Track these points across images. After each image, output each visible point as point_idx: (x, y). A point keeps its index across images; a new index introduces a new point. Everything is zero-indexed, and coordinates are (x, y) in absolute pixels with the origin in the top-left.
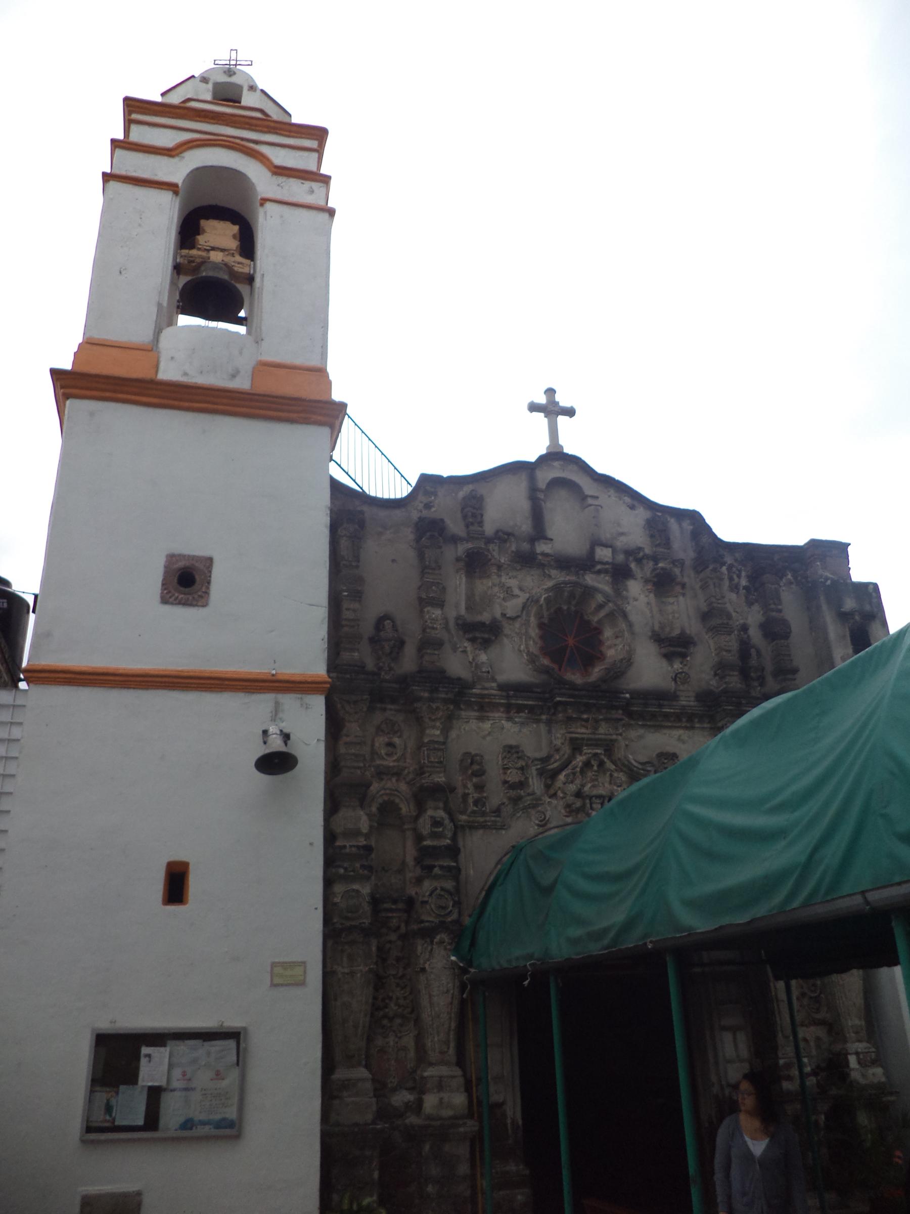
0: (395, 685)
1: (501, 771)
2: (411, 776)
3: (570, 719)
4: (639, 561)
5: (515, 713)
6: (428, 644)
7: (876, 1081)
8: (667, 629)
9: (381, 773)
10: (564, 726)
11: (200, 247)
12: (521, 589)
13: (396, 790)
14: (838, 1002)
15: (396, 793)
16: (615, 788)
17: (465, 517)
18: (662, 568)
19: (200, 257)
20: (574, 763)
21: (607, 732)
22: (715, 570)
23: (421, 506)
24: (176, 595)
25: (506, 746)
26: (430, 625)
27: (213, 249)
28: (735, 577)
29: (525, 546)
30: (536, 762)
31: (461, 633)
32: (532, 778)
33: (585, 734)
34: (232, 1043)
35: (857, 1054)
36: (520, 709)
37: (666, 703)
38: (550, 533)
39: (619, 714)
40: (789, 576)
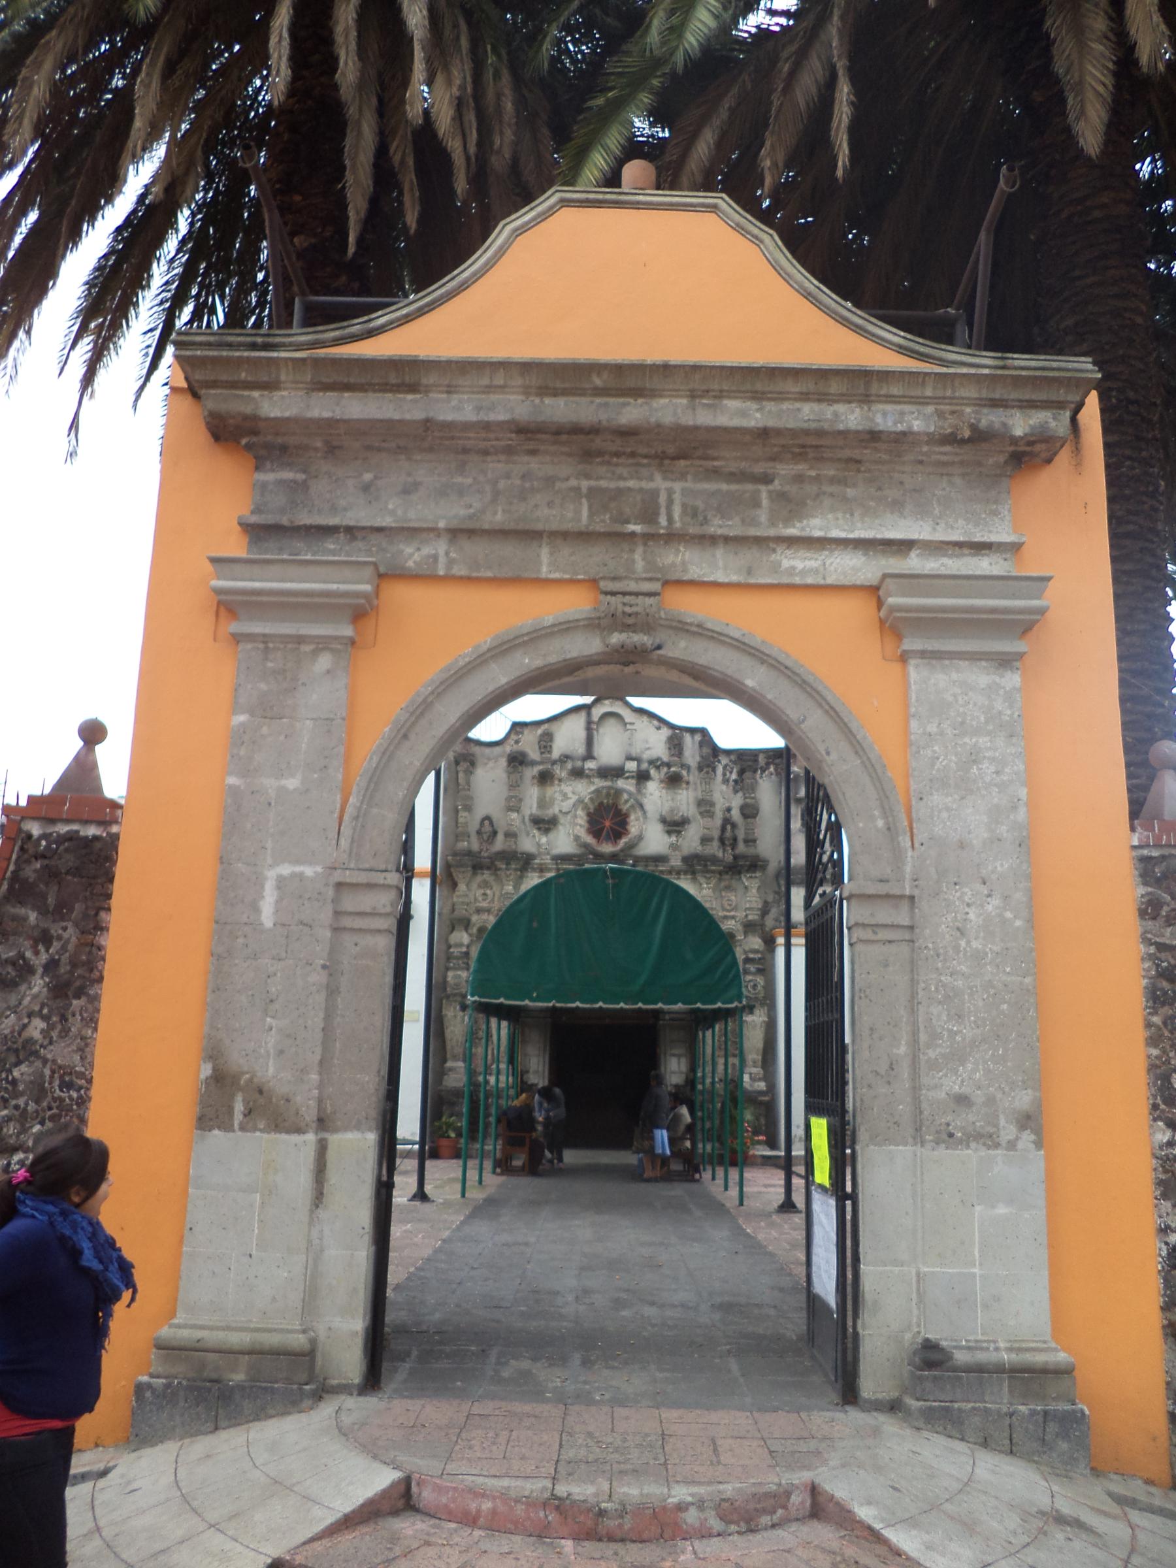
4: (658, 768)
9: (479, 911)
12: (574, 793)
29: (579, 764)
38: (595, 754)
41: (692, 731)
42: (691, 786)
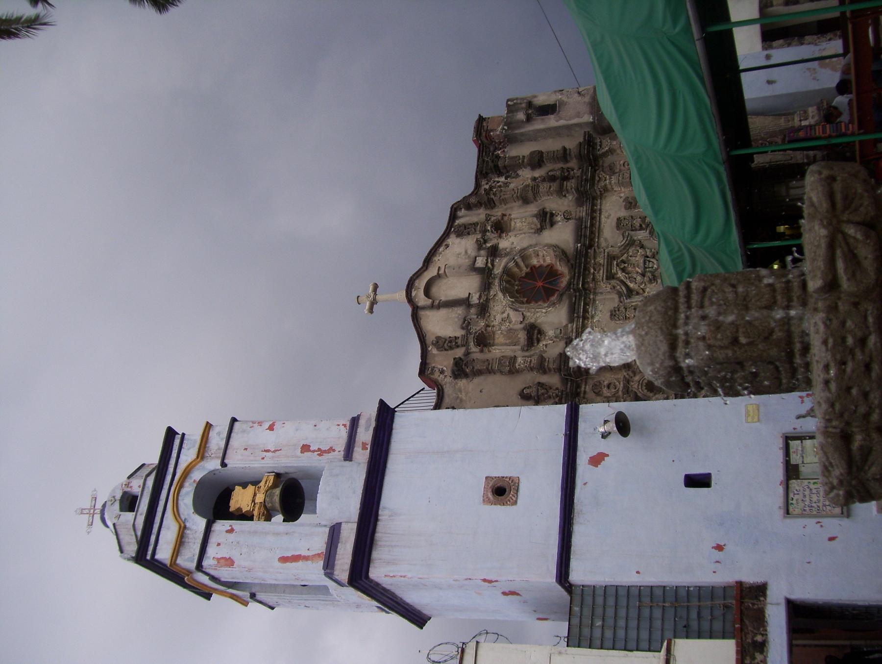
0: (569, 385)
1: (627, 321)
2: (630, 373)
3: (594, 279)
4: (485, 242)
5: (589, 314)
6: (542, 367)
7: (816, 112)
8: (533, 226)
10: (599, 283)
11: (251, 510)
12: (503, 313)
13: (639, 382)
14: (771, 130)
15: (641, 382)
16: (639, 254)
17: (451, 348)
18: (491, 227)
19: (259, 509)
20: (622, 278)
21: (603, 258)
22: (495, 194)
23: (441, 376)
24: (511, 496)
25: (611, 319)
26: (528, 364)
27: (253, 501)
28: (498, 184)
29: (473, 311)
30: (622, 299)
31: (533, 348)
32: (632, 302)
33: (604, 270)
34: (794, 444)
35: (801, 121)
36: (585, 311)
37: (584, 224)
39: (591, 252)
40: (499, 152)
41: (453, 217)
42: (508, 213)
